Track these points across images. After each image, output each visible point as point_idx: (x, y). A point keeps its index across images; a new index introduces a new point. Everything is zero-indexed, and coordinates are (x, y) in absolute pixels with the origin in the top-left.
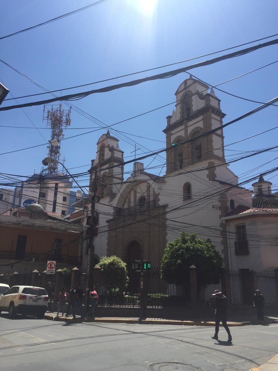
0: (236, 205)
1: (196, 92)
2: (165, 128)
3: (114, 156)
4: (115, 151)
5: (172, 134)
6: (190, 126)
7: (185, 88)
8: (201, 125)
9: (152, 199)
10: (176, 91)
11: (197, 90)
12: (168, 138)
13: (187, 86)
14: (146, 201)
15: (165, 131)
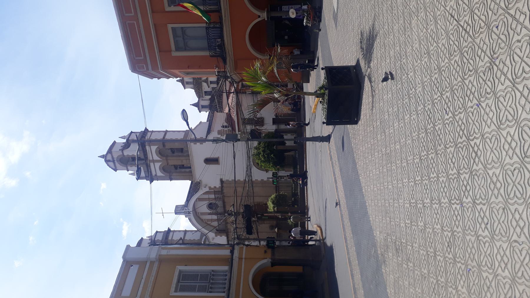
0: (225, 124)
1: (121, 151)
2: (149, 182)
3: (161, 239)
4: (156, 239)
5: (156, 175)
6: (153, 158)
7: (114, 161)
8: (154, 148)
9: (213, 196)
10: (113, 170)
11: (118, 150)
12: (158, 178)
13: (111, 159)
14: (214, 202)
15: (151, 182)
